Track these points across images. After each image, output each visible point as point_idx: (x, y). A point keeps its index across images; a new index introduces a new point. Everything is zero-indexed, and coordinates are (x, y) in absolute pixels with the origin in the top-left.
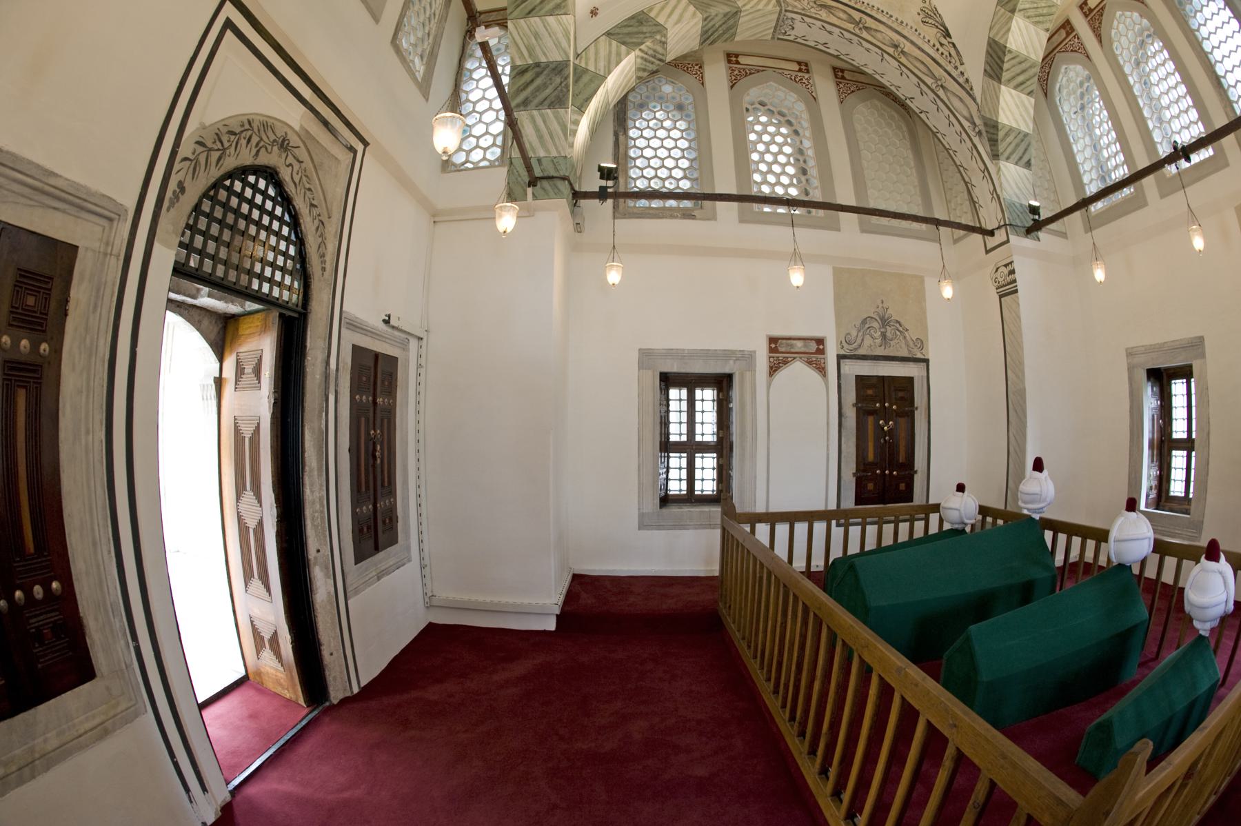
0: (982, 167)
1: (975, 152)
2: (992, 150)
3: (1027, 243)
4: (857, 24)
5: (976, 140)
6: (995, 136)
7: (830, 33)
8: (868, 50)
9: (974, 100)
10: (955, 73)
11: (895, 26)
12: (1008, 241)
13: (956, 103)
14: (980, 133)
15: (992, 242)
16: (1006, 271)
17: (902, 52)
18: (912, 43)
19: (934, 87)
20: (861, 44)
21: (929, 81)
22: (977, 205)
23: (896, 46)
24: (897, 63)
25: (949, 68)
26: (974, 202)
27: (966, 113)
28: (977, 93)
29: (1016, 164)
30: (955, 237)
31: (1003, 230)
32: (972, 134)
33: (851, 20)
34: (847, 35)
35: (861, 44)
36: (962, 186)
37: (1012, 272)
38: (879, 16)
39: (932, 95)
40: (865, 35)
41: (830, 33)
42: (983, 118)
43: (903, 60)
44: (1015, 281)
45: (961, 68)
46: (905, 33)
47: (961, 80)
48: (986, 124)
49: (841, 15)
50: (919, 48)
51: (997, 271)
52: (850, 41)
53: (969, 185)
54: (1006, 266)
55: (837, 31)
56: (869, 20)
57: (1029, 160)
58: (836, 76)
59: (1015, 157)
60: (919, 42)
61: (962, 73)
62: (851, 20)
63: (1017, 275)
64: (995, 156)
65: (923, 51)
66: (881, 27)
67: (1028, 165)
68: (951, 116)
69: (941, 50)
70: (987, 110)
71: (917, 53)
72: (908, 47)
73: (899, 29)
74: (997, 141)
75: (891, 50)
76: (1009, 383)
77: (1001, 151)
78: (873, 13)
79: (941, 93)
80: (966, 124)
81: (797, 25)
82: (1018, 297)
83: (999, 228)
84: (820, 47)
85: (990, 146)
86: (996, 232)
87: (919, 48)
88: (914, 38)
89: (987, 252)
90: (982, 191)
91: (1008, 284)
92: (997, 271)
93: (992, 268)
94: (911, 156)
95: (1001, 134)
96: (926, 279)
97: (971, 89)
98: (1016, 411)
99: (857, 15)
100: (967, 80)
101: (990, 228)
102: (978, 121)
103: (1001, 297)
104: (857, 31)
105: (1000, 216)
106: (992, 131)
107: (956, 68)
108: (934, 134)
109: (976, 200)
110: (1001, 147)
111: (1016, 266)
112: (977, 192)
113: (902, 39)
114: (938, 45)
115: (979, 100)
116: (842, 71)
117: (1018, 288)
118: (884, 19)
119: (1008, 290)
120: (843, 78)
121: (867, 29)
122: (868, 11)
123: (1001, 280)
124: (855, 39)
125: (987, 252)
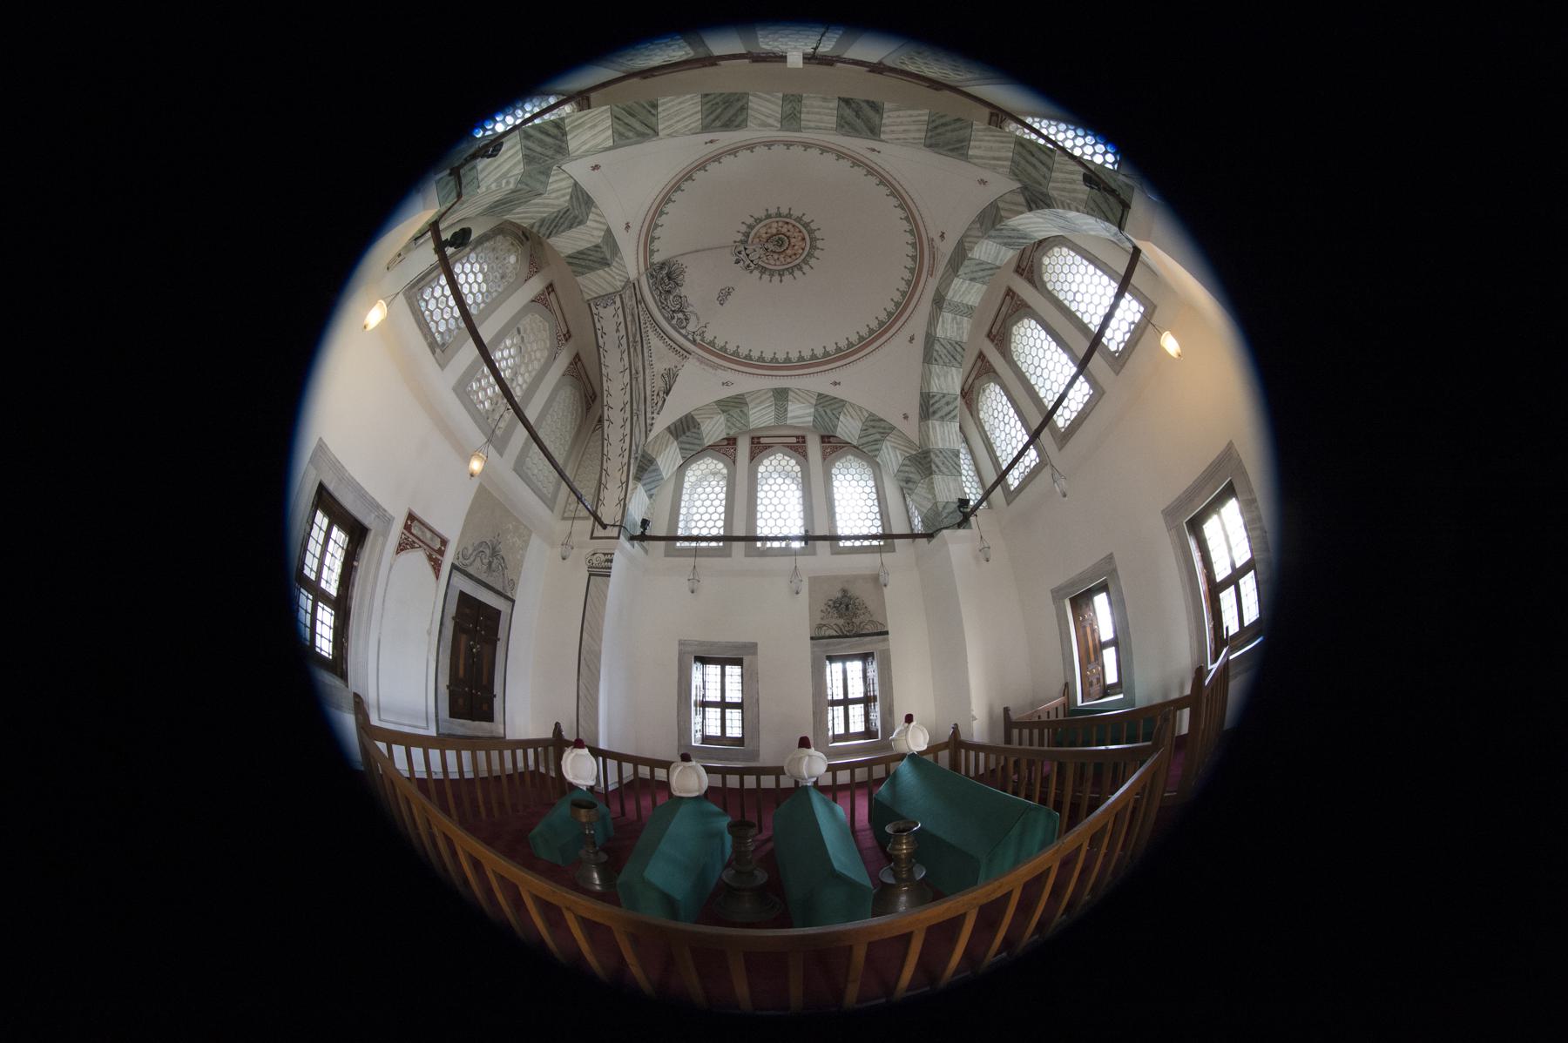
0: (624, 479)
1: (625, 468)
2: (637, 474)
3: (627, 545)
4: (635, 342)
5: (632, 461)
6: (646, 467)
7: (618, 330)
8: (622, 359)
9: (646, 437)
10: (649, 415)
11: (646, 363)
12: (618, 538)
13: (636, 431)
14: (636, 458)
15: (599, 532)
16: (603, 558)
17: (637, 378)
18: (644, 379)
19: (634, 411)
20: (623, 353)
21: (635, 407)
22: (600, 503)
23: (637, 373)
24: (628, 381)
25: (648, 410)
26: (599, 499)
27: (637, 440)
28: (652, 436)
29: (646, 492)
30: (566, 515)
31: (617, 529)
32: (633, 456)
33: (634, 337)
34: (624, 341)
35: (623, 353)
36: (595, 483)
37: (611, 561)
38: (645, 350)
39: (628, 415)
40: (632, 350)
41: (618, 330)
42: (644, 451)
43: (634, 383)
44: (610, 568)
45: (655, 415)
46: (647, 372)
47: (649, 421)
48: (643, 456)
49: (634, 329)
50: (644, 385)
51: (593, 555)
52: (620, 345)
53: (602, 486)
54: (605, 554)
55: (623, 332)
56: (640, 345)
57: (653, 495)
58: (574, 359)
59: (649, 487)
60: (648, 383)
61: (653, 418)
62: (634, 337)
63: (614, 565)
64: (638, 478)
65: (645, 388)
66: (640, 357)
67: (650, 496)
68: (628, 436)
69: (655, 397)
70: (651, 448)
71: (641, 386)
72: (641, 379)
73: (647, 366)
74: (646, 470)
75: (634, 372)
76: (583, 643)
77: (644, 477)
78: (645, 346)
79: (635, 418)
80: (634, 447)
81: (611, 310)
82: (609, 581)
83: (614, 525)
84: (599, 333)
85: (638, 470)
86: (608, 527)
87: (644, 385)
88: (648, 378)
89: (592, 538)
90: (611, 495)
91: (602, 568)
92: (593, 555)
93: (590, 550)
94: (569, 443)
95: (652, 468)
96: (533, 535)
97: (650, 431)
98: (588, 666)
99: (638, 338)
100: (652, 424)
101: (606, 522)
102: (639, 451)
103: (590, 575)
104: (631, 345)
105: (619, 517)
106: (646, 462)
107: (653, 413)
108: (603, 439)
109: (602, 498)
110: (645, 476)
111: (615, 558)
112: (605, 494)
113: (642, 372)
114: (656, 393)
115: (649, 440)
116: (579, 360)
117: (612, 574)
118: (646, 355)
119: (600, 571)
120: (576, 363)
121: (635, 349)
122: (644, 342)
123: (594, 562)
124: (625, 346)
125: (592, 538)
